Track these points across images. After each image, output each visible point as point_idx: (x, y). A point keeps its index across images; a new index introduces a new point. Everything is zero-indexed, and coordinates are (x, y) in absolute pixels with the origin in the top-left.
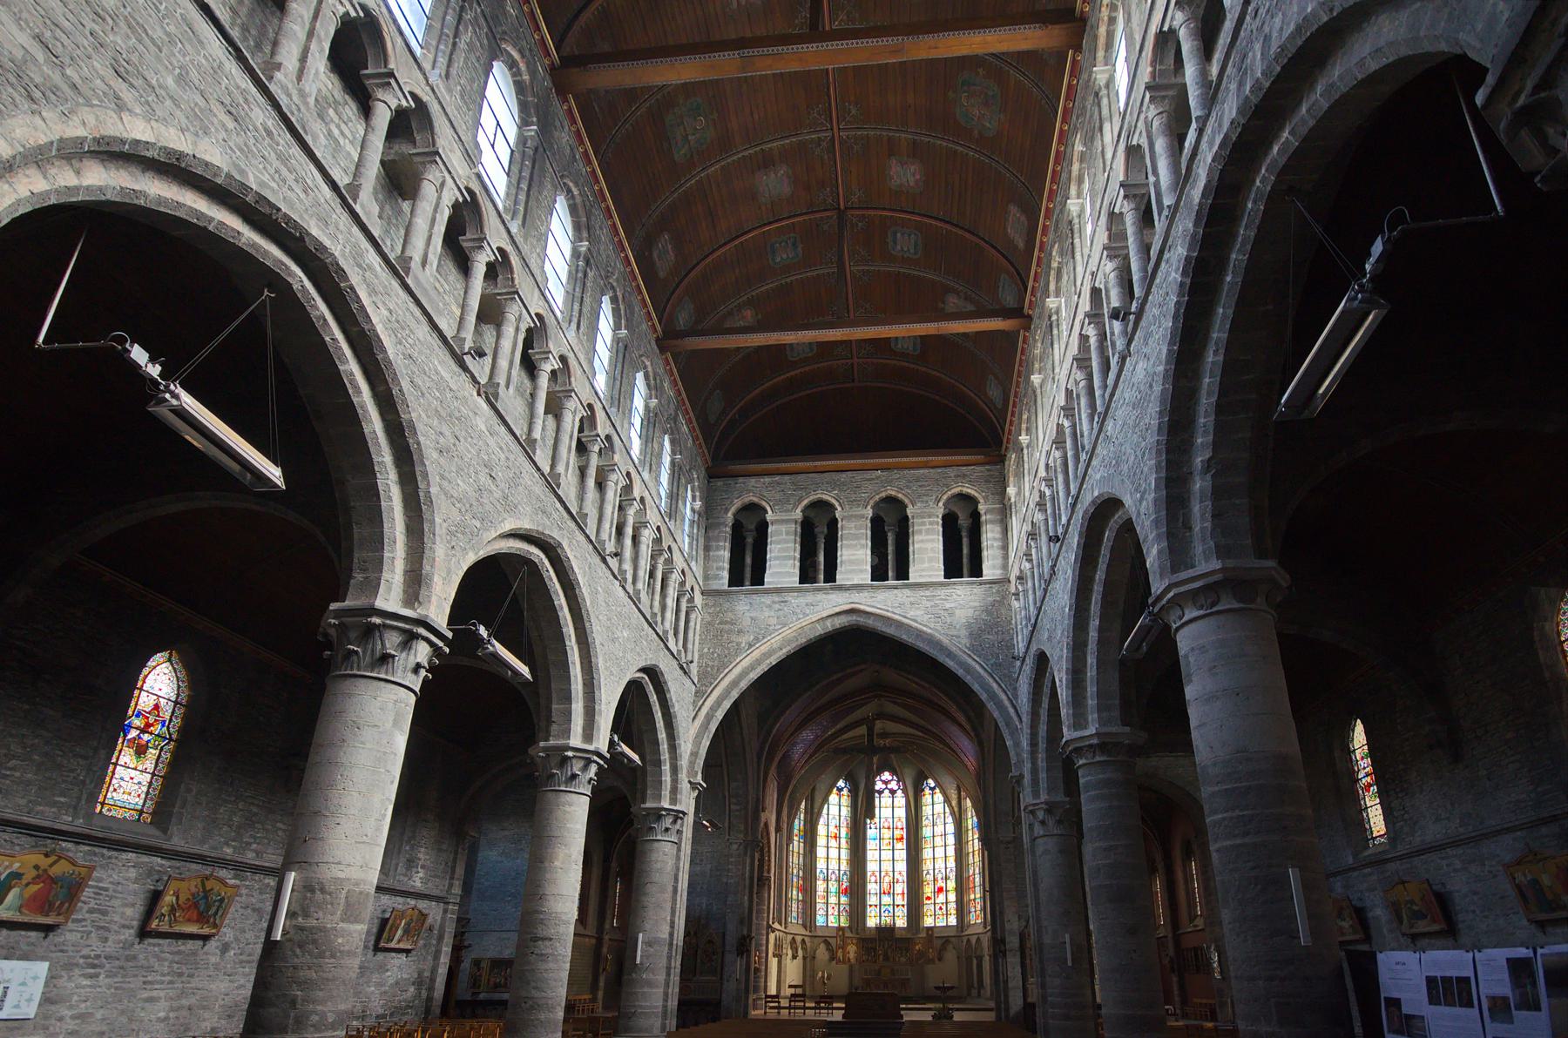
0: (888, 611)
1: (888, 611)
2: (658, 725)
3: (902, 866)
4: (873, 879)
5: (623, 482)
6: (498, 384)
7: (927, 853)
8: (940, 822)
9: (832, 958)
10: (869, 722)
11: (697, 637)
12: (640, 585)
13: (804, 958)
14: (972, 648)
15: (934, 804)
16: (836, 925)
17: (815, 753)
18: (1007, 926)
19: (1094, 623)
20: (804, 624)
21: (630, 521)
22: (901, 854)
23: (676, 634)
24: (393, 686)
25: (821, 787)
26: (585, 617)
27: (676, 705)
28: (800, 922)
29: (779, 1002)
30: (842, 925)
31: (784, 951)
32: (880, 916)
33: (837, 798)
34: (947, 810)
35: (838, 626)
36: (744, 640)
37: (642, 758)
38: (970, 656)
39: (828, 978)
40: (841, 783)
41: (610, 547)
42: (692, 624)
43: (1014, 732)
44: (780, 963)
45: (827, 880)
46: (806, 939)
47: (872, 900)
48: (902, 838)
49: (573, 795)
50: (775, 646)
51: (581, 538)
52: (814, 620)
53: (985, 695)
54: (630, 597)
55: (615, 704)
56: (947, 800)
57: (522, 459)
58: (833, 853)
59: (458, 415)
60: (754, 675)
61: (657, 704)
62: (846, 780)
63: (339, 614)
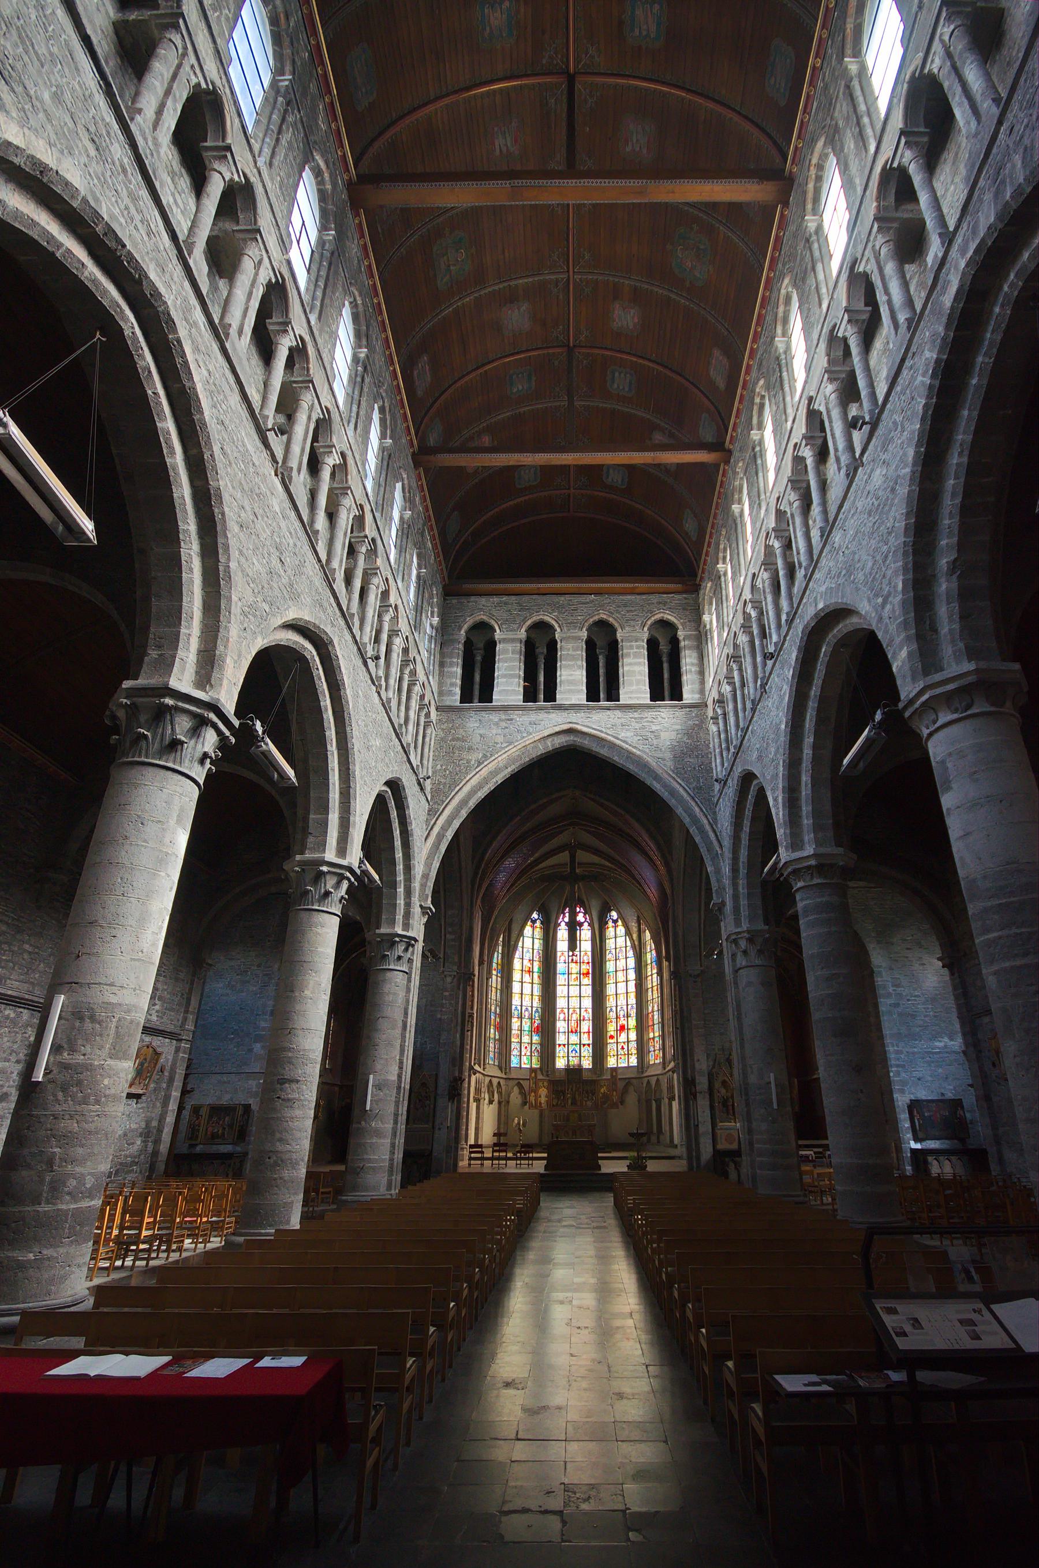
0: (601, 731)
1: (601, 731)
3: (587, 1003)
4: (562, 1016)
5: (382, 588)
6: (292, 468)
7: (610, 990)
8: (622, 956)
9: (524, 1103)
10: (571, 848)
11: (431, 754)
12: (391, 695)
14: (677, 771)
15: (617, 937)
18: (697, 1065)
19: (809, 740)
20: (527, 743)
21: (386, 627)
22: (587, 991)
23: (416, 747)
24: (180, 777)
26: (347, 722)
27: (413, 822)
29: (482, 1152)
30: (534, 1066)
32: (568, 1057)
34: (629, 944)
36: (474, 757)
38: (674, 779)
39: (524, 1125)
40: (535, 915)
41: (370, 652)
42: (427, 739)
45: (521, 1018)
46: (502, 1082)
47: (561, 1039)
48: (588, 973)
50: (501, 765)
51: (349, 637)
52: (537, 738)
53: (688, 820)
54: (383, 705)
55: (366, 817)
56: (628, 933)
57: (307, 548)
58: (527, 989)
59: (257, 491)
60: (481, 794)
61: (397, 821)
63: (132, 692)
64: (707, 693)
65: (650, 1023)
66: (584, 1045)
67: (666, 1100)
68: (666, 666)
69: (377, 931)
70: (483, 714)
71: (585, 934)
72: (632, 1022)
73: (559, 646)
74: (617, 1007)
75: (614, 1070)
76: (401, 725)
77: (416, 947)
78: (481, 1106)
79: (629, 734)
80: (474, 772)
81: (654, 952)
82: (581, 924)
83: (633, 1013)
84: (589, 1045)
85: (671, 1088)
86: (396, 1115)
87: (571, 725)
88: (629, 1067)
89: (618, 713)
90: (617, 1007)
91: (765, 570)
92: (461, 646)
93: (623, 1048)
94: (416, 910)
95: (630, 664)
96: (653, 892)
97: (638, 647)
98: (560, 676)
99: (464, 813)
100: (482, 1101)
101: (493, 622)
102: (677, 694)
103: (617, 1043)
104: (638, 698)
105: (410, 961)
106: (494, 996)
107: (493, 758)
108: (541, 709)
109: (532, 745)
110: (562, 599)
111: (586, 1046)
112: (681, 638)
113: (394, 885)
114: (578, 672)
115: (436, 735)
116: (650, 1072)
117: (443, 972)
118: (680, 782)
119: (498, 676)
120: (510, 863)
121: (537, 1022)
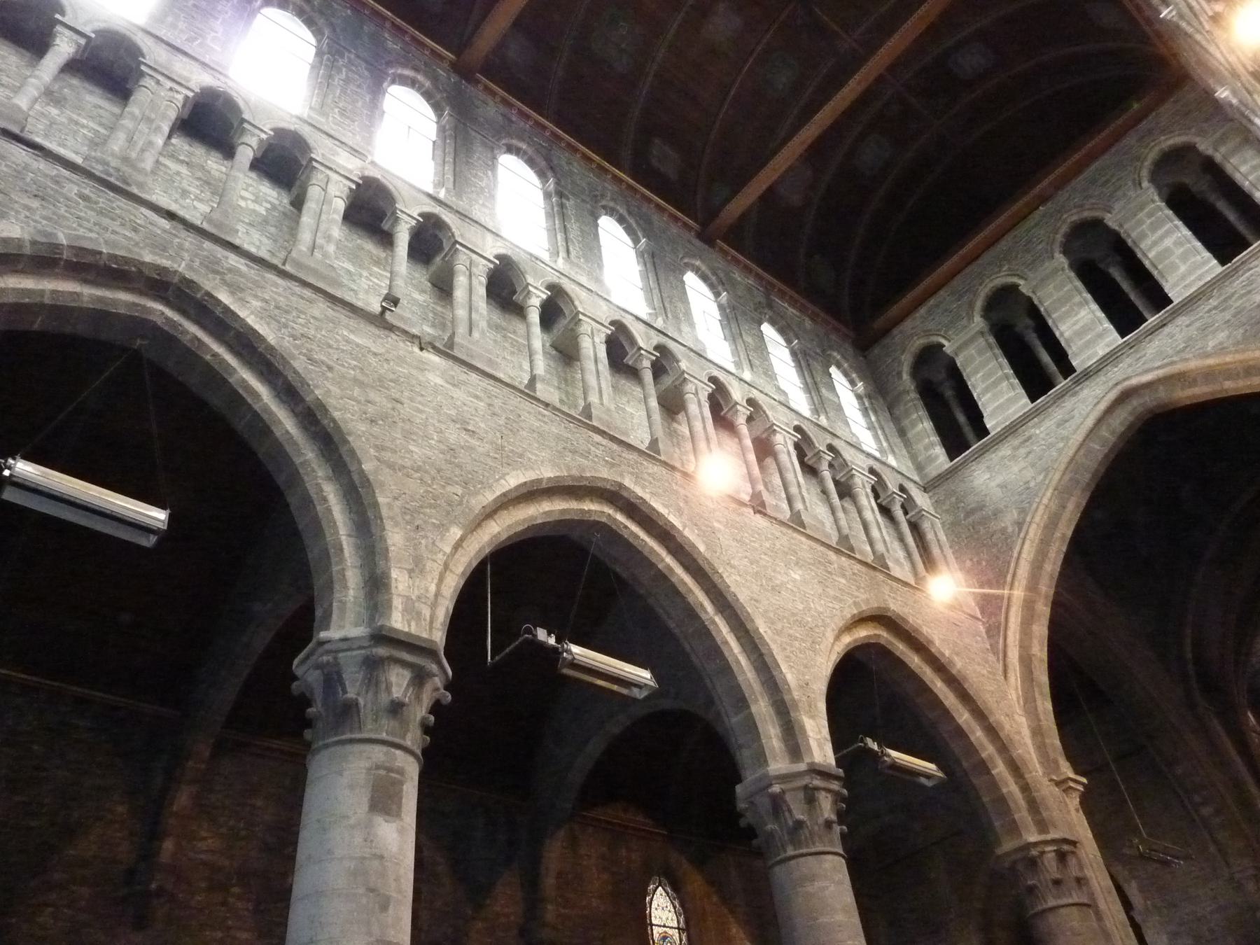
2: (947, 703)
27: (956, 659)
68: (1222, 206)
70: (988, 456)
73: (1036, 302)
79: (1222, 336)
80: (1020, 541)
87: (1120, 388)
89: (1182, 320)
92: (914, 395)
94: (1047, 791)
95: (1155, 243)
105: (1081, 882)
107: (1035, 505)
108: (1061, 396)
109: (1082, 452)
110: (1003, 245)
112: (1210, 152)
115: (943, 524)
119: (978, 395)
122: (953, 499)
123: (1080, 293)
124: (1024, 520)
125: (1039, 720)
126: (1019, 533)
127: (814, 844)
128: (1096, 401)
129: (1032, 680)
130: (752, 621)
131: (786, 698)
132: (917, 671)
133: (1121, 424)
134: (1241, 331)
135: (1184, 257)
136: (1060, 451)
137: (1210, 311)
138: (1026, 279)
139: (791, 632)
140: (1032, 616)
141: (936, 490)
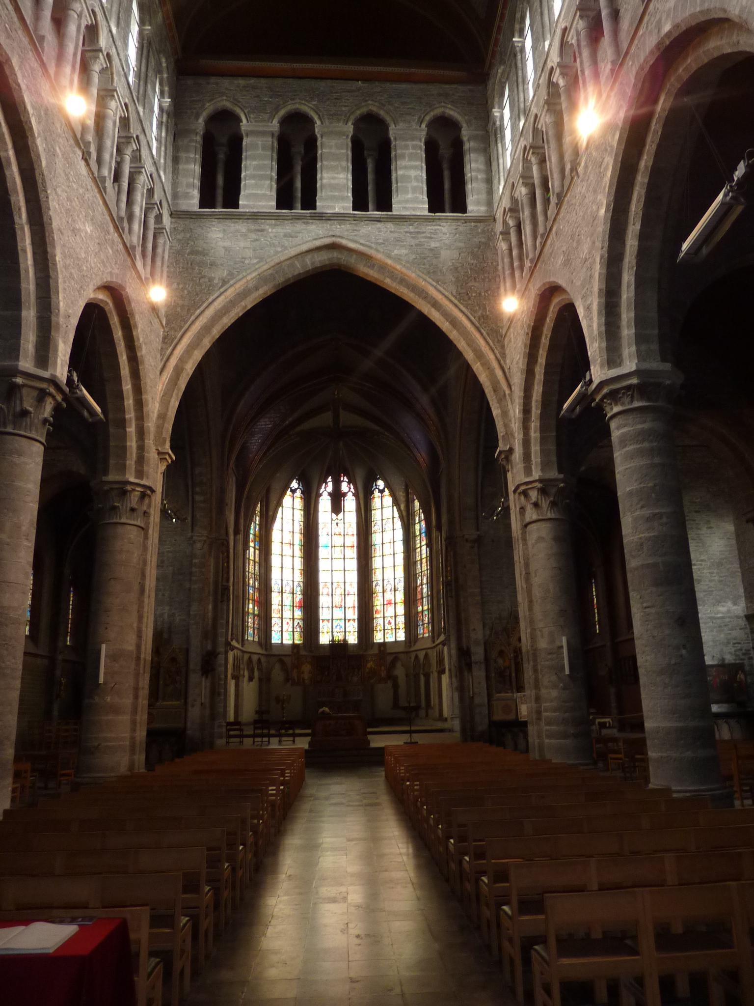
2: (122, 372)
3: (353, 577)
7: (377, 563)
8: (388, 526)
9: (287, 680)
13: (260, 680)
16: (291, 642)
17: (268, 450)
22: (352, 565)
25: (276, 486)
27: (144, 347)
28: (256, 639)
29: (241, 730)
30: (297, 642)
31: (242, 672)
32: (332, 632)
33: (291, 499)
34: (396, 514)
35: (318, 264)
37: (103, 411)
43: (501, 399)
44: (237, 685)
46: (263, 659)
49: (24, 440)
50: (250, 285)
56: (396, 502)
58: (288, 561)
60: (227, 321)
62: (299, 481)
64: (495, 205)
65: (419, 596)
66: (349, 620)
67: (436, 674)
68: (446, 174)
69: (105, 479)
70: (228, 222)
71: (350, 503)
72: (400, 596)
73: (319, 143)
74: (383, 580)
75: (380, 644)
76: (122, 219)
77: (153, 498)
78: (240, 683)
79: (404, 251)
81: (423, 524)
82: (345, 495)
83: (401, 586)
84: (354, 620)
85: (441, 661)
86: (136, 689)
88: (396, 642)
89: (390, 226)
90: (383, 580)
91: (581, 17)
92: (199, 138)
93: (390, 623)
94: (152, 455)
95: (406, 168)
96: (422, 456)
97: (414, 147)
98: (321, 179)
99: (207, 344)
100: (241, 678)
101: (238, 110)
102: (460, 206)
103: (384, 617)
104: (414, 209)
106: (252, 568)
107: (241, 276)
108: (298, 218)
109: (288, 262)
110: (322, 85)
111: (352, 622)
112: (465, 139)
113: (122, 423)
114: (342, 176)
115: (171, 247)
116: (419, 646)
117: (192, 537)
118: (464, 309)
119: (246, 176)
120: (265, 424)
121: (299, 597)
122: (188, 235)
123: (347, 161)
124: (228, 281)
125: (167, 409)
126: (220, 288)
127: (31, 430)
128: (316, 237)
129: (176, 384)
130: (54, 247)
131: (53, 319)
132: (116, 341)
133: (320, 261)
134: (414, 256)
135: (415, 190)
136: (277, 253)
137: (406, 232)
138: (322, 123)
139: (73, 271)
140: (198, 345)
141: (179, 221)
